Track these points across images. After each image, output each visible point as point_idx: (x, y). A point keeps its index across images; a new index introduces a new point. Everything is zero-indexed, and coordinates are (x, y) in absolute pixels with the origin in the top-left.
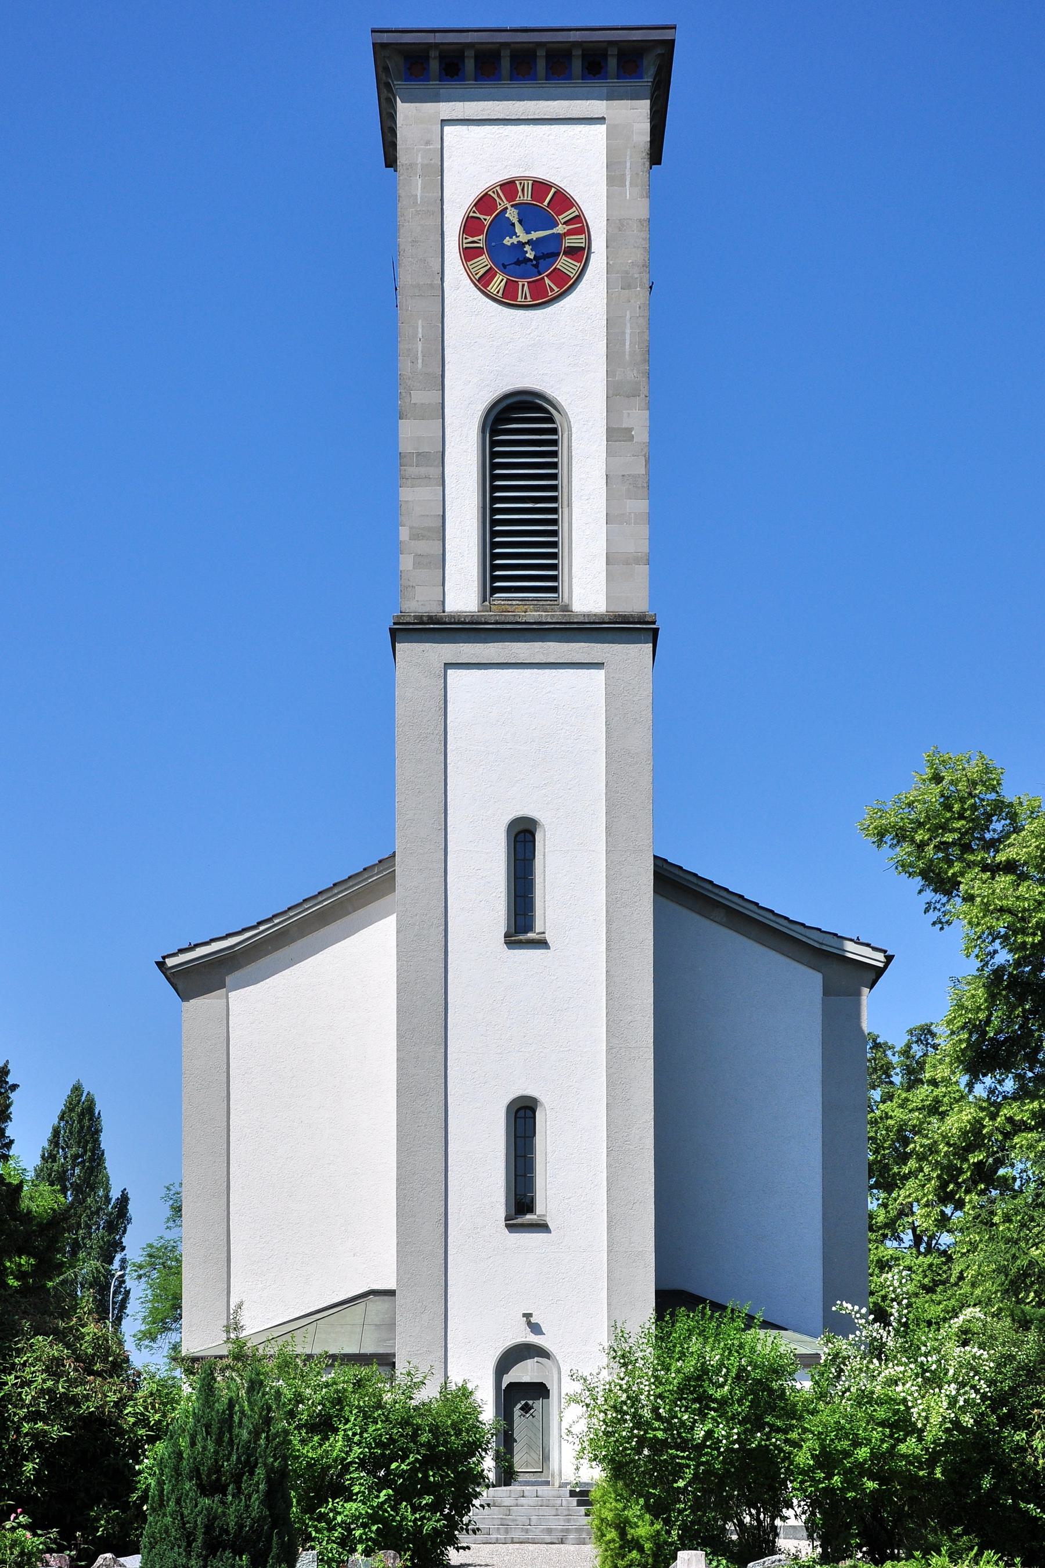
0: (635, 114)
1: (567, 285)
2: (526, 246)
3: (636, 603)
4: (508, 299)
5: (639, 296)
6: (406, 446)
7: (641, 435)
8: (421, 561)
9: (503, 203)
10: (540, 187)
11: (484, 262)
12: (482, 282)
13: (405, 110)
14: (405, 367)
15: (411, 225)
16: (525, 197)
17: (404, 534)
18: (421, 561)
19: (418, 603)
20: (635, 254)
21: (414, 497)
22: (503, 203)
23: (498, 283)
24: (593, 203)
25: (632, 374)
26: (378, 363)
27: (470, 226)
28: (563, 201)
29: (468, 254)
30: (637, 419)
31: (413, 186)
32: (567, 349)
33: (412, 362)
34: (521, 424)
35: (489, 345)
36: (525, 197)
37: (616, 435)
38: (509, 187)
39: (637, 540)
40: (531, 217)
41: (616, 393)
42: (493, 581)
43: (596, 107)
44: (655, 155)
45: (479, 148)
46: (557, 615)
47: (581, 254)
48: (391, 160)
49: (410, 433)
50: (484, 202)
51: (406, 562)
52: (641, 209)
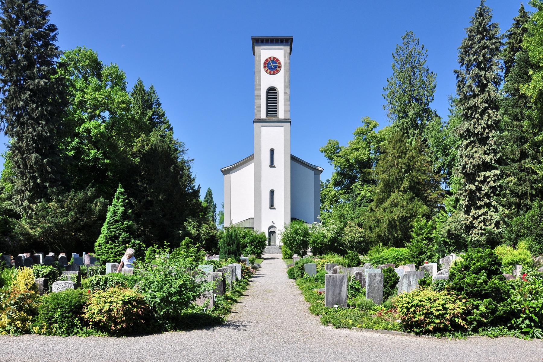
0: (288, 48)
1: (278, 72)
2: (273, 66)
3: (288, 117)
4: (270, 73)
5: (288, 73)
6: (256, 94)
7: (289, 93)
8: (258, 111)
9: (269, 60)
10: (274, 58)
11: (267, 68)
12: (266, 71)
13: (256, 47)
14: (255, 83)
15: (257, 63)
17: (255, 107)
18: (258, 111)
19: (257, 117)
20: (288, 67)
21: (257, 101)
22: (269, 60)
23: (269, 71)
24: (282, 60)
25: (287, 84)
26: (252, 82)
27: (265, 63)
28: (278, 60)
29: (265, 67)
30: (288, 91)
31: (257, 58)
32: (278, 81)
33: (256, 83)
34: (272, 92)
35: (267, 80)
37: (285, 93)
38: (270, 58)
39: (288, 108)
40: (273, 62)
41: (285, 87)
42: (268, 114)
43: (282, 47)
44: (290, 54)
45: (266, 53)
46: (277, 119)
47: (280, 67)
48: (254, 54)
49: (256, 92)
50: (267, 60)
51: (256, 111)
52: (288, 61)
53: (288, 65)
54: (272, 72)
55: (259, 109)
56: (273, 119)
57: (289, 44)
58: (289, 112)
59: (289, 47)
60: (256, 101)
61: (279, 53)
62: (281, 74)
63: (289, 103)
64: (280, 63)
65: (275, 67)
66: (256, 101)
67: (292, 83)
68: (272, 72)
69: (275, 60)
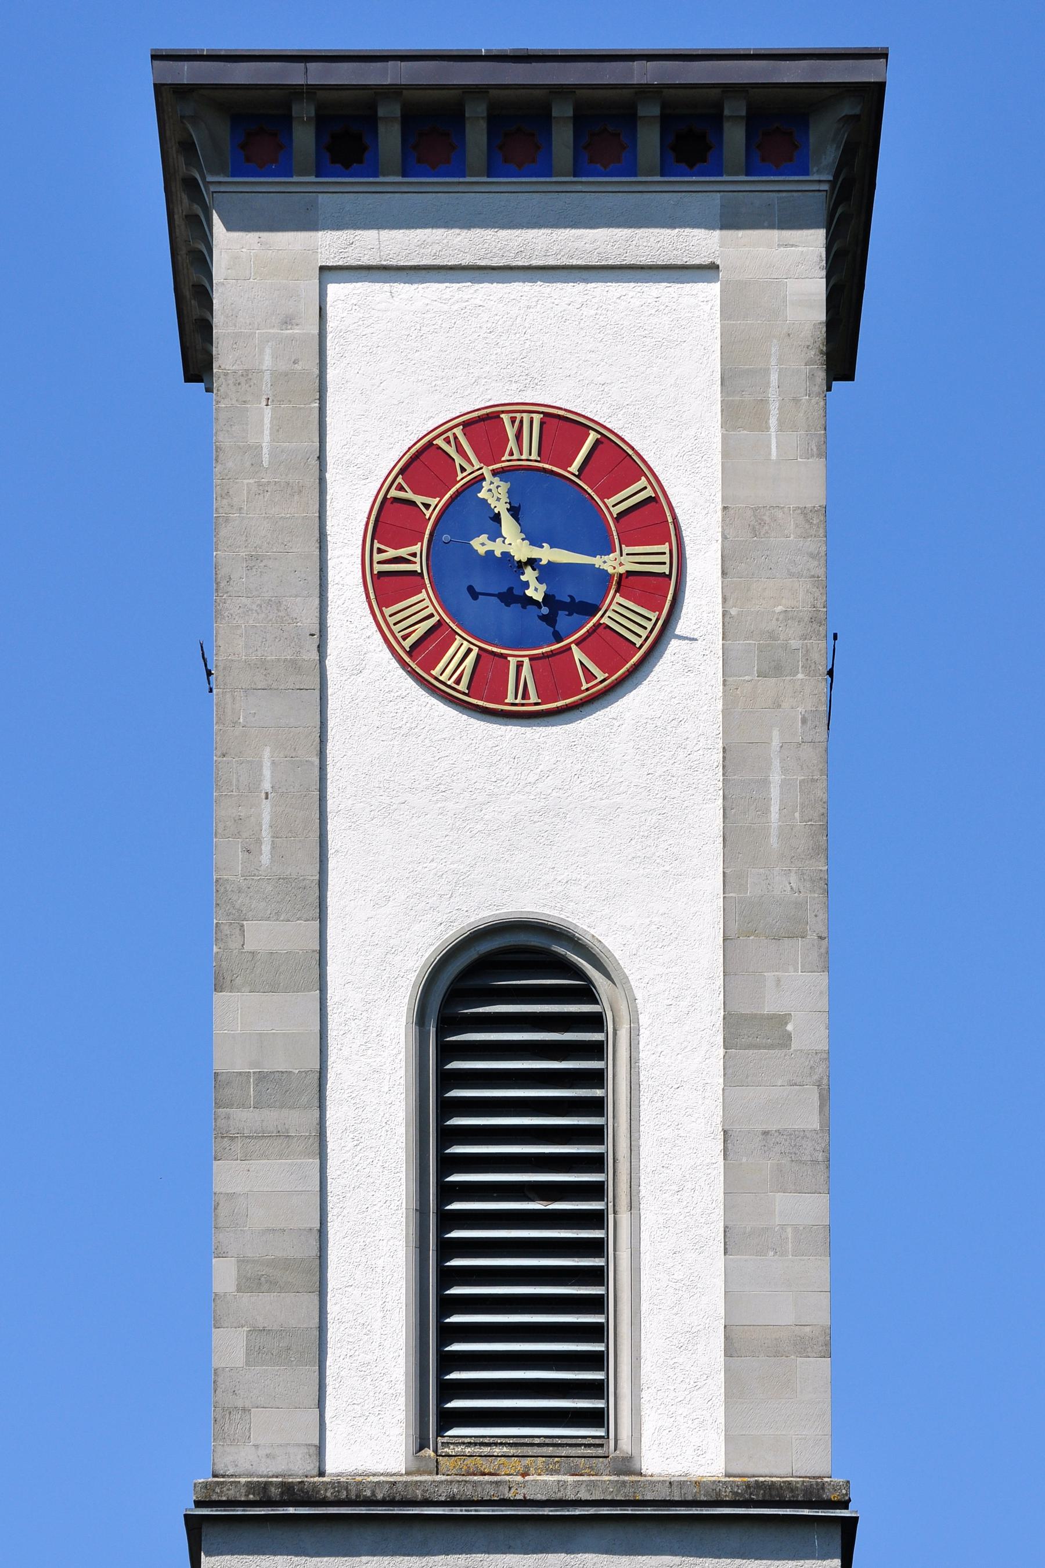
1: (627, 664)
2: (527, 571)
3: (798, 1452)
4: (483, 697)
5: (804, 692)
6: (231, 1058)
7: (810, 1032)
8: (267, 1347)
9: (469, 464)
10: (561, 428)
11: (424, 606)
12: (420, 656)
13: (230, 247)
14: (230, 862)
15: (248, 515)
16: (618, 612)
17: (224, 1276)
18: (267, 1347)
19: (260, 1453)
20: (789, 593)
21: (251, 1183)
22: (469, 464)
23: (458, 659)
24: (689, 469)
25: (783, 884)
26: (160, 842)
27: (389, 521)
28: (616, 461)
29: (386, 588)
30: (799, 994)
31: (249, 421)
32: (625, 825)
33: (250, 841)
34: (514, 1006)
35: (432, 816)
36: (618, 612)
37: (747, 1031)
38: (484, 428)
39: (801, 1294)
40: (540, 500)
41: (746, 929)
42: (444, 1399)
43: (699, 243)
44: (840, 356)
45: (408, 334)
46: (602, 1483)
47: (660, 591)
48: (198, 365)
49: (243, 1025)
50: (424, 464)
51: (229, 1348)
52: (804, 483)
53: (796, 548)
54: (520, 666)
55: (291, 1310)
56: (544, 1482)
57: (818, 180)
58: (817, 1370)
59: (811, 244)
60: (230, 1176)
61: (651, 338)
62: (686, 687)
63: (811, 1208)
64: (653, 520)
65: (571, 602)
66: (230, 1176)
67: (856, 864)
68: (520, 666)
69: (577, 472)
